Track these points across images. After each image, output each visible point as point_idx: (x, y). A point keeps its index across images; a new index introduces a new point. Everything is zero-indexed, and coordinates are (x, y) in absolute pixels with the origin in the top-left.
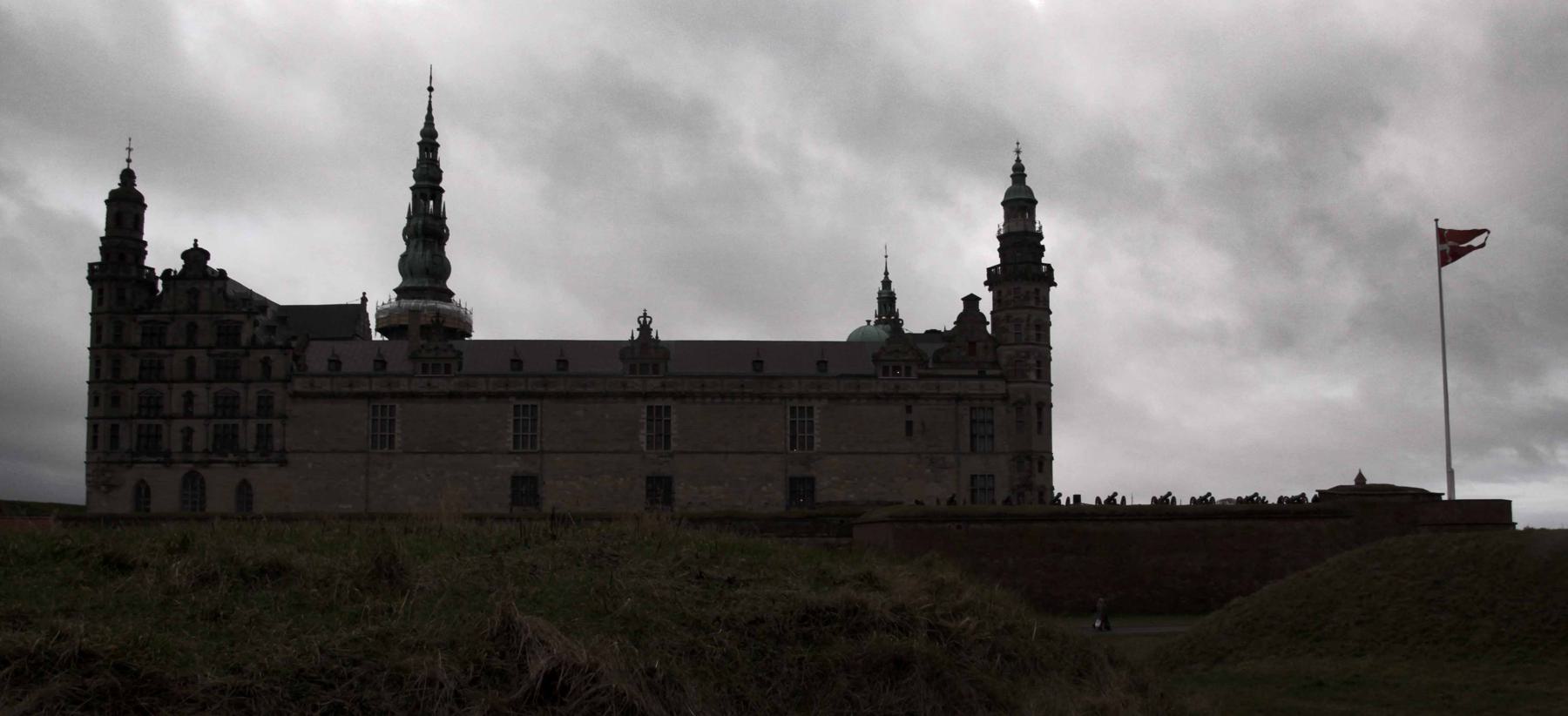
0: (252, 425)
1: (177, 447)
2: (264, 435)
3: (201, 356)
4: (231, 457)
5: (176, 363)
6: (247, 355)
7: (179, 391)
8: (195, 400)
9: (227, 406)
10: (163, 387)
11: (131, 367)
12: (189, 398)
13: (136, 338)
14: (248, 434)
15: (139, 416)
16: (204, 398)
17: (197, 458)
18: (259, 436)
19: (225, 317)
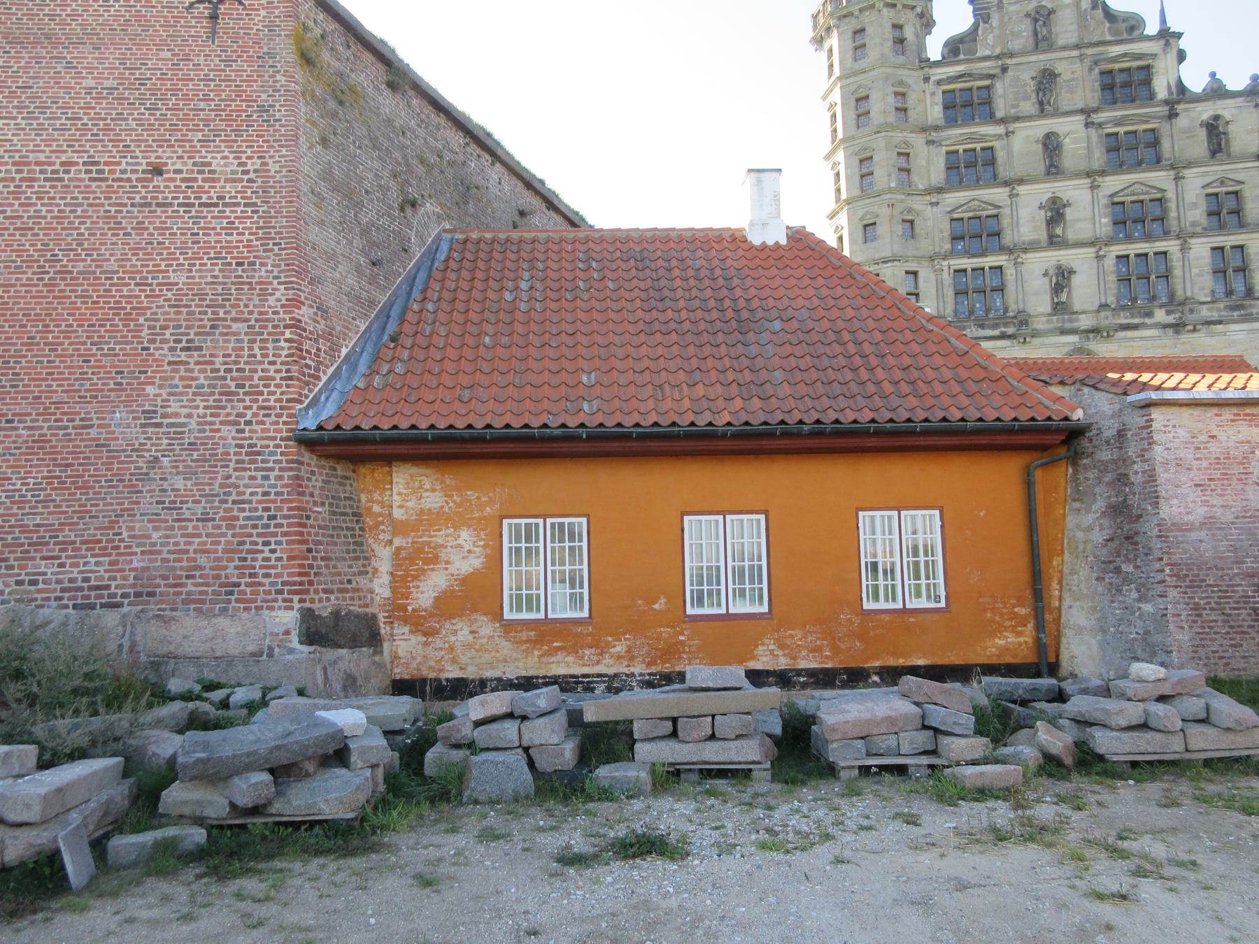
0: (1201, 249)
1: (1039, 303)
2: (1231, 267)
3: (1071, 130)
4: (1160, 316)
5: (1020, 146)
6: (1172, 115)
7: (1033, 197)
8: (1069, 213)
9: (1135, 218)
10: (998, 194)
11: (930, 165)
12: (1056, 212)
13: (936, 113)
14: (1194, 265)
15: (952, 254)
16: (1086, 208)
17: (1085, 322)
18: (1220, 272)
19: (1116, 50)
